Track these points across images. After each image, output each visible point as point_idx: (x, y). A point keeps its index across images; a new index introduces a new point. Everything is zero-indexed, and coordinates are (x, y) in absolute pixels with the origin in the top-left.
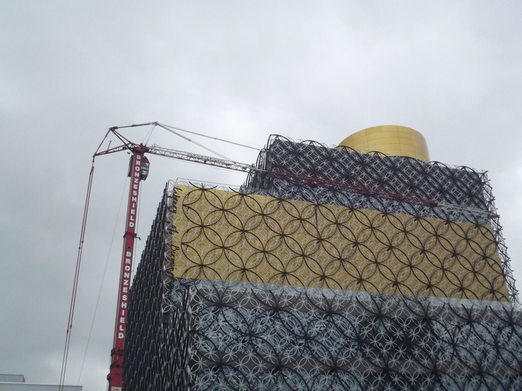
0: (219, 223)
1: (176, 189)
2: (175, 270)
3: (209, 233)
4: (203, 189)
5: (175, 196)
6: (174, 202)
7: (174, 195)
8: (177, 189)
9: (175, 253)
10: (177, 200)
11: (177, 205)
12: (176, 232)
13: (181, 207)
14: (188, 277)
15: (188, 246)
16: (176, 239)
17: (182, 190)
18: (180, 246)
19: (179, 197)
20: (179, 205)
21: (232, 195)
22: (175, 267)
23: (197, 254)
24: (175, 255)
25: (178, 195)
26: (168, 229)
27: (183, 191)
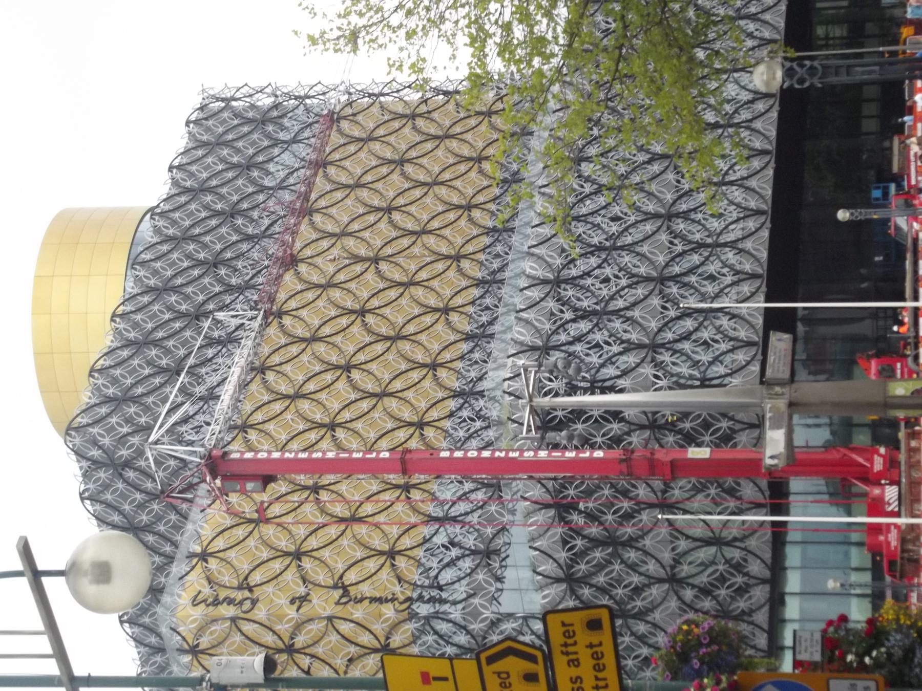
3: (313, 543)
6: (229, 604)
10: (224, 600)
22: (390, 597)
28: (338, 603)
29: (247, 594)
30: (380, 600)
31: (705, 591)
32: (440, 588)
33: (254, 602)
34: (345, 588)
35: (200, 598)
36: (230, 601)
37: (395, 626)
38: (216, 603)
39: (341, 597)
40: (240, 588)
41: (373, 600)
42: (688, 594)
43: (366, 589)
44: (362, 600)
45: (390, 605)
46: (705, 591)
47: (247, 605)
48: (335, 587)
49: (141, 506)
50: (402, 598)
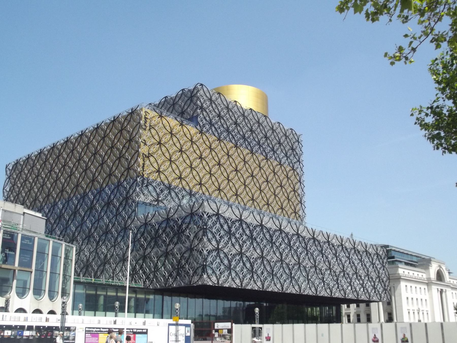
6: (145, 122)
14: (151, 178)
15: (152, 156)
16: (143, 150)
20: (148, 125)
28: (143, 154)
29: (148, 128)
30: (143, 167)
31: (141, 267)
32: (147, 186)
33: (145, 129)
34: (148, 157)
35: (147, 114)
36: (146, 122)
37: (135, 171)
38: (146, 118)
39: (146, 155)
40: (150, 126)
41: (144, 164)
42: (141, 262)
43: (147, 162)
44: (144, 161)
45: (142, 169)
46: (141, 267)
47: (144, 127)
48: (149, 154)
49: (180, 106)
50: (144, 173)
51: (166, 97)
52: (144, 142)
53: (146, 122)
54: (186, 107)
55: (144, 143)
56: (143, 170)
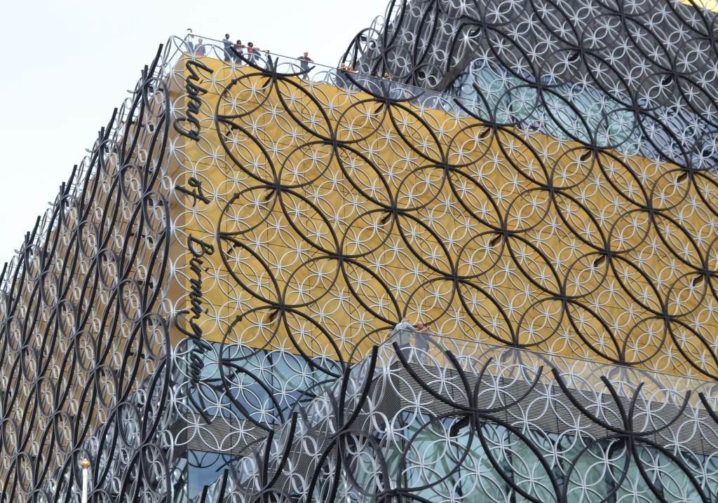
0: (321, 183)
1: (193, 67)
2: (202, 314)
4: (270, 74)
5: (194, 87)
6: (190, 105)
7: (190, 84)
8: (197, 65)
9: (200, 263)
10: (198, 101)
11: (199, 117)
12: (201, 197)
13: (213, 125)
14: (241, 337)
17: (211, 72)
18: (214, 243)
19: (205, 92)
20: (205, 117)
21: (355, 101)
22: (203, 307)
23: (264, 273)
24: (203, 267)
25: (201, 86)
26: (177, 188)
27: (215, 74)
28: (191, 239)
30: (196, 293)
33: (194, 136)
41: (197, 285)
43: (213, 279)
44: (197, 271)
50: (201, 322)
51: (359, 37)
52: (190, 189)
53: (193, 109)
54: (424, 43)
55: (193, 194)
56: (197, 311)
